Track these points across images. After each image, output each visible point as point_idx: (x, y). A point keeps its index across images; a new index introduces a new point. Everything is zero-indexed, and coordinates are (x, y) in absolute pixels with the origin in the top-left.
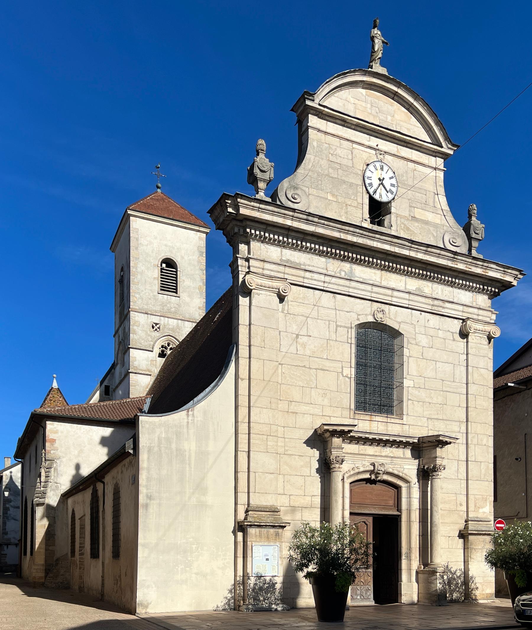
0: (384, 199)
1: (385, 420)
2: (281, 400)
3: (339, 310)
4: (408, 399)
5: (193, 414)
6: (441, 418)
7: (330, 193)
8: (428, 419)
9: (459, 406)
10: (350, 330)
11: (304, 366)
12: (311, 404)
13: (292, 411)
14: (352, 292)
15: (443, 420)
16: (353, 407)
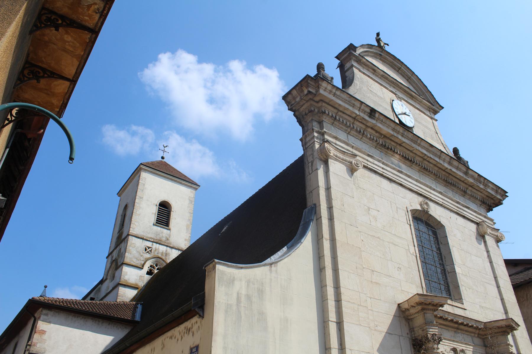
5: (276, 271)
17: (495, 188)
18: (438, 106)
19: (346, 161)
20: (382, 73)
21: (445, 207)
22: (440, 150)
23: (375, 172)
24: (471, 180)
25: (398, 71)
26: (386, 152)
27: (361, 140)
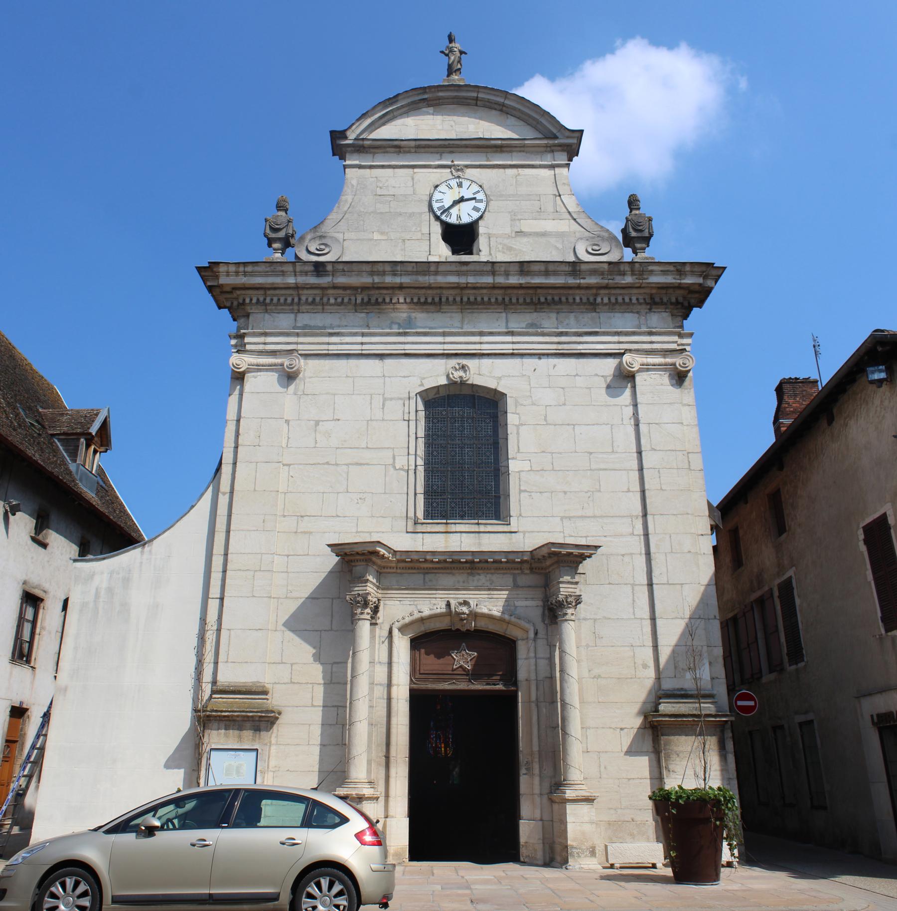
0: (466, 220)
1: (475, 528)
2: (284, 516)
4: (521, 491)
5: (150, 551)
6: (591, 514)
8: (562, 518)
9: (629, 491)
10: (407, 403)
11: (327, 463)
15: (594, 517)
16: (420, 514)
17: (672, 268)
18: (567, 134)
19: (275, 365)
21: (522, 355)
22: (488, 262)
24: (592, 280)
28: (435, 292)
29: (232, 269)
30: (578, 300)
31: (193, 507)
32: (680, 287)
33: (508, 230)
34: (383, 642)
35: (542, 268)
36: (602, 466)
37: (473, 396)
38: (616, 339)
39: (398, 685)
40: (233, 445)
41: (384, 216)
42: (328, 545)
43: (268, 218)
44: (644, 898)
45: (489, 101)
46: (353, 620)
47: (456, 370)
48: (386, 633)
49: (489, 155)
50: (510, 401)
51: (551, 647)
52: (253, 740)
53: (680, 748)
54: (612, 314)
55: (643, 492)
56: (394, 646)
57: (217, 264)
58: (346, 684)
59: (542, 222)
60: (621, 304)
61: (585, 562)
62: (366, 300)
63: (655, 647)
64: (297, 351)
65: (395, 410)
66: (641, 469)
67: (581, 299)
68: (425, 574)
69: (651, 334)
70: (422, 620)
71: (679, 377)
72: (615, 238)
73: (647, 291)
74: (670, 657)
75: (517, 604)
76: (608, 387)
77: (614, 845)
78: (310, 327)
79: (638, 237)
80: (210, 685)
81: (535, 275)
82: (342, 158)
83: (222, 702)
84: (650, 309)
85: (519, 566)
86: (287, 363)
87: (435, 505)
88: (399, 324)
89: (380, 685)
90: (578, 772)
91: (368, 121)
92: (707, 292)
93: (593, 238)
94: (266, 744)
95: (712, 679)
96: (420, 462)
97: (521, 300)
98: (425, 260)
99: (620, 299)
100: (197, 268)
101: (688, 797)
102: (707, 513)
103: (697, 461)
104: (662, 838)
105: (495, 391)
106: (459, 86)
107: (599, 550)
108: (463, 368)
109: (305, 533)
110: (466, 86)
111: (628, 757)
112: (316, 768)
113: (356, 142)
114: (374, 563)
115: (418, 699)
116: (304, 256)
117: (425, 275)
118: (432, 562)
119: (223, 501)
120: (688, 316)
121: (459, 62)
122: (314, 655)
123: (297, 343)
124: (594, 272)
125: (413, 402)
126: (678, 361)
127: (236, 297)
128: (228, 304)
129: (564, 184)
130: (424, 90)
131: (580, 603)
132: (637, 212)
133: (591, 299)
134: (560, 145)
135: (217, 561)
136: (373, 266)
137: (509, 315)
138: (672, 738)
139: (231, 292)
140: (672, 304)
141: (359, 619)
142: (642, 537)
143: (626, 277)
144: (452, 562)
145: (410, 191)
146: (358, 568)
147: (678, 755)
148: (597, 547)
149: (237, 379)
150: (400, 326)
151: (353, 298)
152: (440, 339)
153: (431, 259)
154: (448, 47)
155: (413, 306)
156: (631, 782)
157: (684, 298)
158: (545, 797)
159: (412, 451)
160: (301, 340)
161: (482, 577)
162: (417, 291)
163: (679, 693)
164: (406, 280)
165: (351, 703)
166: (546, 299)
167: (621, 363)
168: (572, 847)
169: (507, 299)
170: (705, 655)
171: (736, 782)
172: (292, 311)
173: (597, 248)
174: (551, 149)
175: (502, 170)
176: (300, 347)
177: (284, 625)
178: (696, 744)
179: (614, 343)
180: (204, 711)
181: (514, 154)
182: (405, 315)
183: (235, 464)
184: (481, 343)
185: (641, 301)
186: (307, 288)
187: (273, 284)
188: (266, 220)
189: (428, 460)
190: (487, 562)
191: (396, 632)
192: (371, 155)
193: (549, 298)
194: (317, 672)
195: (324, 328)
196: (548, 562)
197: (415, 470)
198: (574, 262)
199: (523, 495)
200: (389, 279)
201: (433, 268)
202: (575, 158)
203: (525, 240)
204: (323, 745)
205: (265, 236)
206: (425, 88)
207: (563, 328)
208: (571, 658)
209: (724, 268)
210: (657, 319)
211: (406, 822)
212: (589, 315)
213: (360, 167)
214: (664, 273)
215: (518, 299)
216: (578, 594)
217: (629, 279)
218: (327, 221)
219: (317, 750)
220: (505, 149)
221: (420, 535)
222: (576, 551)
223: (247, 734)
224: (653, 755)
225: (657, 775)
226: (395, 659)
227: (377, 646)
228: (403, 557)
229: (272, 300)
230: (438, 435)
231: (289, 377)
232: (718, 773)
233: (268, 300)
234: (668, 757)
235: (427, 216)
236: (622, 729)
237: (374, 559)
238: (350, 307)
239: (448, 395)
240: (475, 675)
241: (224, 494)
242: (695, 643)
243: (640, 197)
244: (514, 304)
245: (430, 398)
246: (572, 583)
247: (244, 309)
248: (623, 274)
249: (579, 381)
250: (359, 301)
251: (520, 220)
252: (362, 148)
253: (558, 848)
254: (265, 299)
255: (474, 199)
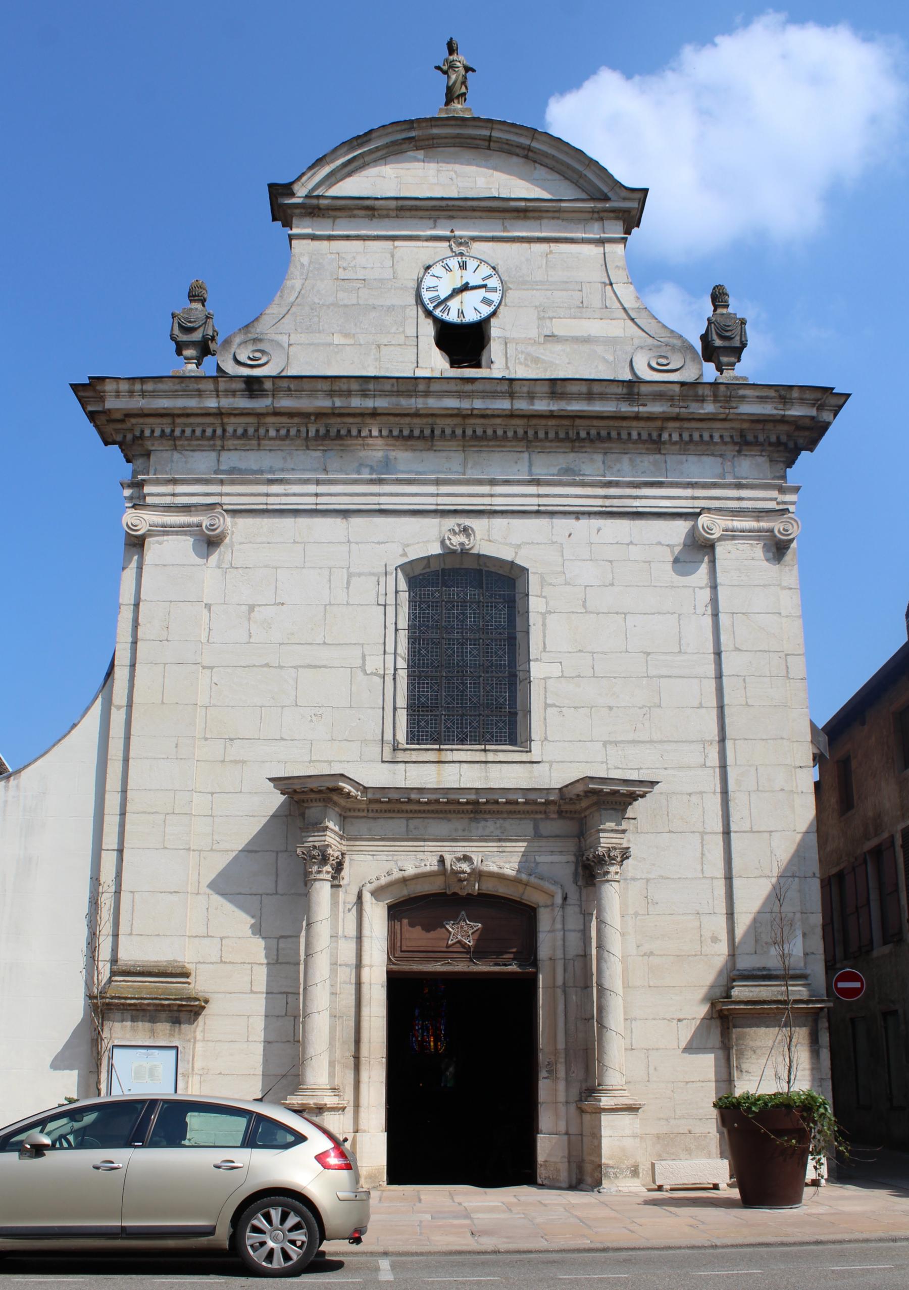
0: (471, 317)
1: (481, 756)
2: (206, 739)
3: (357, 543)
4: (547, 706)
6: (646, 738)
7: (341, 332)
8: (605, 744)
9: (701, 706)
10: (382, 580)
11: (267, 665)
12: (282, 739)
13: (233, 759)
14: (387, 502)
15: (651, 742)
16: (402, 737)
18: (625, 194)
19: (189, 526)
20: (393, 204)
21: (552, 514)
22: (503, 379)
23: (296, 512)
25: (489, 148)
26: (340, 445)
27: (259, 448)
28: (424, 420)
29: (124, 386)
30: (635, 435)
31: (75, 725)
32: (783, 420)
33: (533, 333)
34: (349, 910)
35: (584, 388)
36: (664, 672)
37: (481, 571)
38: (689, 492)
39: (371, 966)
40: (130, 640)
41: (350, 310)
42: (270, 779)
43: (177, 312)
44: (701, 1227)
45: (508, 142)
46: (307, 881)
47: (455, 533)
48: (354, 899)
49: (507, 223)
50: (533, 580)
51: (586, 916)
52: (172, 1035)
53: (758, 1043)
54: (684, 458)
55: (721, 708)
56: (365, 914)
57: (102, 379)
58: (299, 964)
59: (585, 323)
60: (697, 443)
61: (636, 803)
62: (322, 431)
63: (731, 915)
64: (221, 505)
65: (366, 590)
66: (719, 676)
67: (639, 434)
68: (408, 819)
69: (739, 486)
70: (404, 881)
71: (778, 549)
72: (691, 348)
73: (736, 425)
74: (750, 927)
75: (538, 859)
76: (676, 561)
77: (663, 1163)
78: (239, 471)
79: (724, 348)
80: (109, 965)
81: (571, 399)
82: (287, 224)
83: (125, 986)
84: (739, 451)
85: (543, 808)
86: (206, 522)
87: (422, 724)
88: (372, 467)
89: (346, 965)
90: (618, 1075)
91: (326, 170)
92: (824, 427)
93: (659, 347)
94: (189, 1041)
95: (806, 954)
96: (402, 664)
97: (552, 435)
98: (410, 375)
99: (696, 436)
100: (71, 385)
101: (766, 1104)
102: (809, 738)
103: (798, 667)
104: (728, 1152)
105: (512, 564)
106: (463, 119)
107: (657, 787)
108: (466, 530)
109: (236, 762)
110: (474, 119)
111: (686, 1055)
112: (260, 1071)
113: (308, 201)
114: (335, 804)
115: (397, 984)
116: (231, 368)
117: (411, 396)
118: (419, 802)
119: (118, 718)
120: (793, 462)
121: (464, 83)
122: (252, 926)
123: (221, 495)
124: (659, 397)
125: (391, 579)
126: (777, 526)
127: (131, 427)
128: (119, 438)
129: (617, 267)
130: (410, 124)
131: (627, 858)
132: (724, 311)
133: (655, 435)
134: (613, 211)
135: (112, 801)
136: (333, 384)
137: (534, 456)
138: (748, 1030)
139: (122, 421)
140: (770, 444)
141: (316, 880)
142: (717, 770)
143: (705, 405)
144: (447, 803)
145: (388, 274)
146: (313, 810)
147: (755, 1052)
148: (653, 783)
149: (134, 545)
150: (372, 470)
151: (303, 429)
152: (432, 489)
153: (420, 373)
154: (447, 60)
155: (391, 441)
156: (689, 1085)
157: (789, 436)
158: (573, 1107)
159: (390, 648)
160: (227, 489)
161: (490, 824)
162: (397, 419)
163: (760, 973)
164: (381, 403)
165: (305, 989)
166: (588, 434)
167: (694, 528)
168: (608, 1166)
169: (531, 433)
170: (798, 924)
171: (829, 1083)
172: (213, 448)
173: (664, 361)
174: (599, 216)
175: (525, 246)
176: (225, 500)
177: (213, 886)
178: (779, 1037)
179: (686, 498)
180: (102, 998)
181: (545, 222)
182: (380, 454)
183: (133, 666)
184: (492, 496)
185: (727, 439)
186: (235, 415)
187: (185, 408)
188: (173, 316)
189: (413, 661)
190: (497, 802)
191: (367, 897)
192: (330, 221)
193: (593, 432)
194: (257, 949)
195: (261, 472)
196: (584, 804)
197: (395, 675)
198: (630, 381)
199: (549, 710)
200: (356, 402)
201: (422, 387)
202: (635, 231)
203: (558, 347)
204: (267, 1042)
205: (172, 338)
206: (411, 122)
207: (612, 475)
208: (613, 931)
209: (848, 395)
210: (749, 466)
211: (383, 1137)
212: (651, 458)
213: (314, 237)
214: (762, 399)
215: (546, 433)
216: (625, 846)
217: (709, 408)
218: (264, 316)
219: (261, 1047)
220: (531, 214)
221: (402, 766)
222: (623, 789)
223: (163, 1027)
224: (721, 1053)
225: (725, 1076)
226: (366, 932)
227: (341, 915)
228: (377, 796)
229: (183, 431)
230: (427, 626)
231: (210, 542)
232: (807, 1073)
233: (177, 432)
234: (740, 1054)
235: (413, 311)
236: (679, 1020)
237: (335, 798)
238: (298, 442)
239: (443, 570)
240: (478, 952)
241: (119, 708)
242: (783, 909)
243: (728, 290)
244: (541, 441)
245: (417, 572)
246: (616, 831)
247: (142, 445)
248: (702, 400)
249: (635, 552)
250: (312, 433)
251: (551, 318)
252: (315, 209)
253: (588, 1167)
254: (173, 431)
255: (485, 286)
